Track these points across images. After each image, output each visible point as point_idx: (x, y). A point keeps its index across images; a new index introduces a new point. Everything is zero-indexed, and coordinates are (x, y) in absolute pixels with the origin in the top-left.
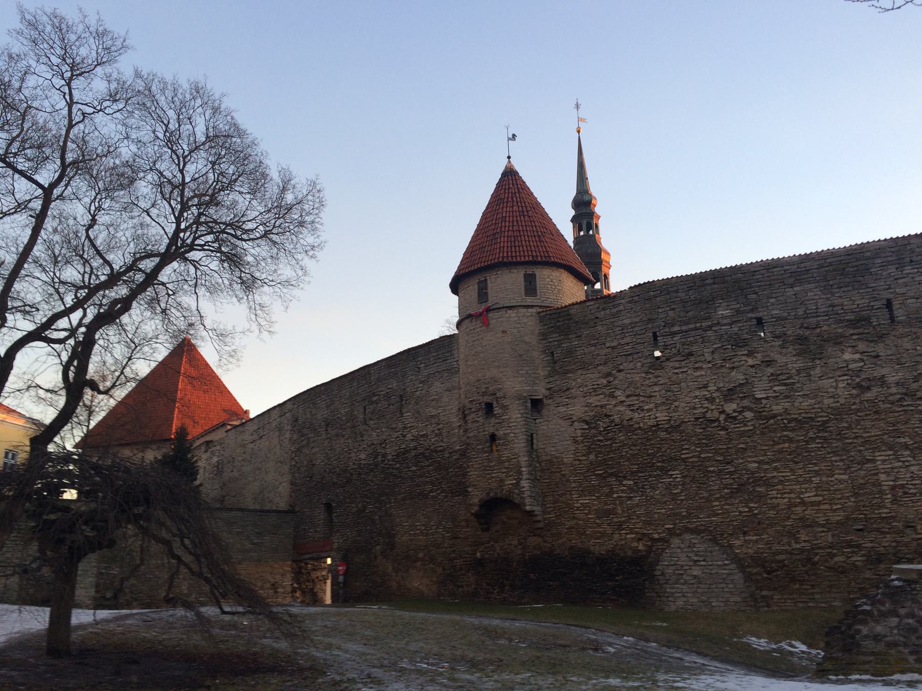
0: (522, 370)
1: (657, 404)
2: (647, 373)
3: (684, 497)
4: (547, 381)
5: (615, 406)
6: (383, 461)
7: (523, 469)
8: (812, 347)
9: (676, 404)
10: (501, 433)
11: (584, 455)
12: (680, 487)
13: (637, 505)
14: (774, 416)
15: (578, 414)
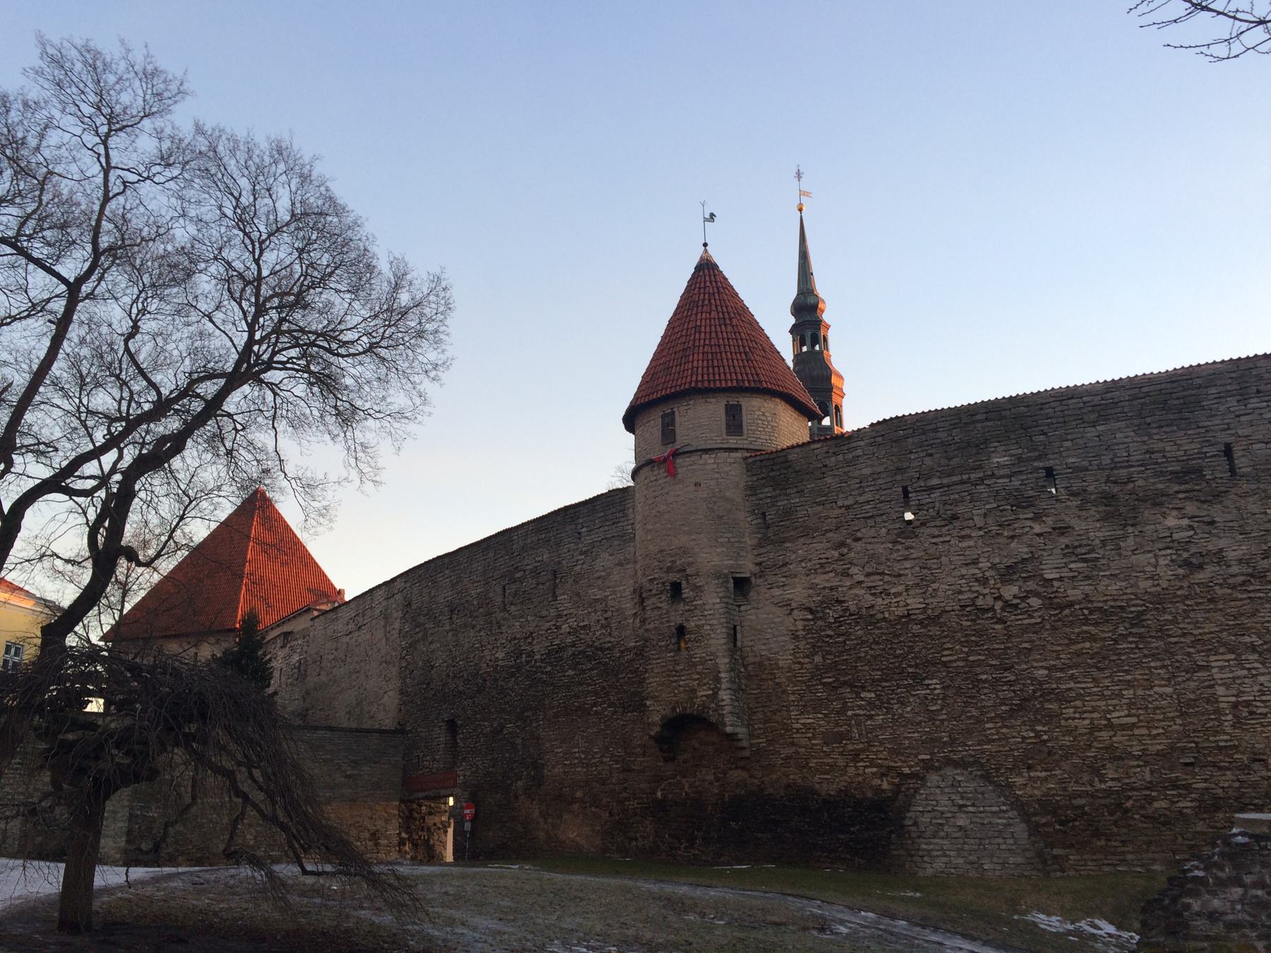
0: (722, 537)
1: (907, 586)
2: (895, 542)
3: (945, 717)
4: (756, 552)
5: (850, 588)
6: (528, 662)
7: (722, 675)
8: (1122, 509)
9: (935, 586)
10: (693, 624)
11: (808, 657)
12: (940, 702)
13: (880, 727)
14: (1071, 604)
15: (799, 599)
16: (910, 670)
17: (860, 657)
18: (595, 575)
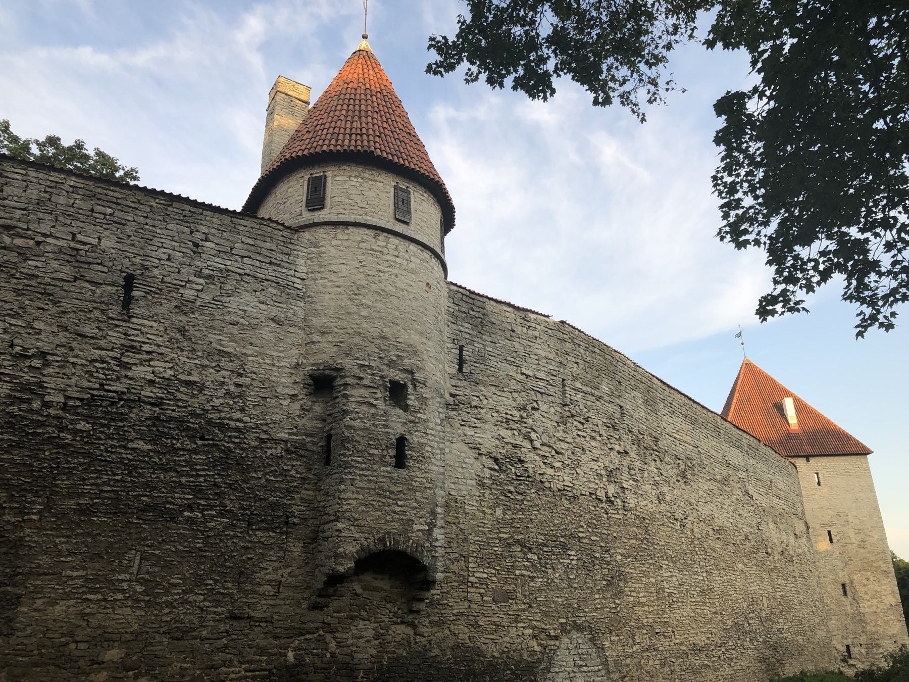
7: (439, 510)
15: (487, 445)
16: (562, 540)
17: (531, 520)
18: (227, 317)
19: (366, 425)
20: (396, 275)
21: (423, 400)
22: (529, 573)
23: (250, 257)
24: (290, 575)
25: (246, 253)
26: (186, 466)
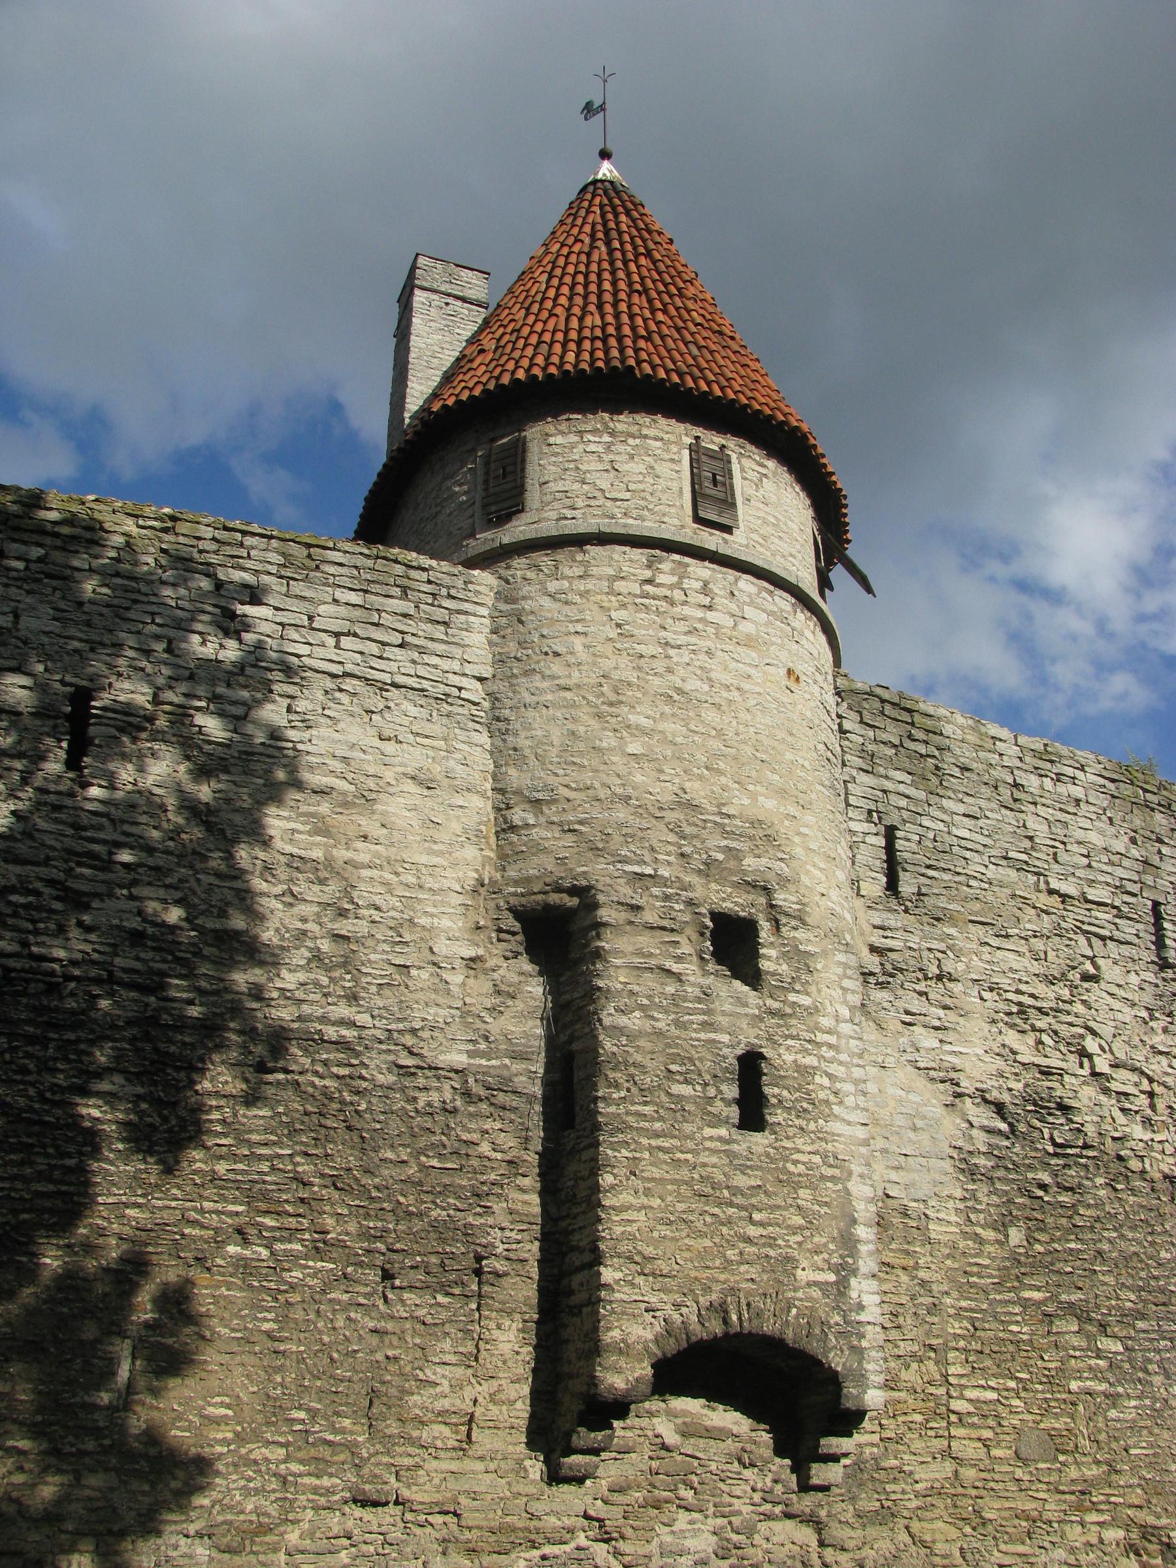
10: (789, 1058)
15: (976, 1074)
17: (1099, 1253)
19: (659, 1025)
20: (709, 653)
21: (799, 958)
22: (1103, 1387)
23: (355, 635)
24: (492, 1398)
25: (344, 626)
26: (224, 1135)
